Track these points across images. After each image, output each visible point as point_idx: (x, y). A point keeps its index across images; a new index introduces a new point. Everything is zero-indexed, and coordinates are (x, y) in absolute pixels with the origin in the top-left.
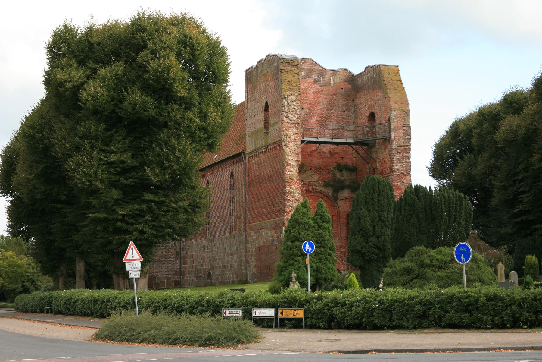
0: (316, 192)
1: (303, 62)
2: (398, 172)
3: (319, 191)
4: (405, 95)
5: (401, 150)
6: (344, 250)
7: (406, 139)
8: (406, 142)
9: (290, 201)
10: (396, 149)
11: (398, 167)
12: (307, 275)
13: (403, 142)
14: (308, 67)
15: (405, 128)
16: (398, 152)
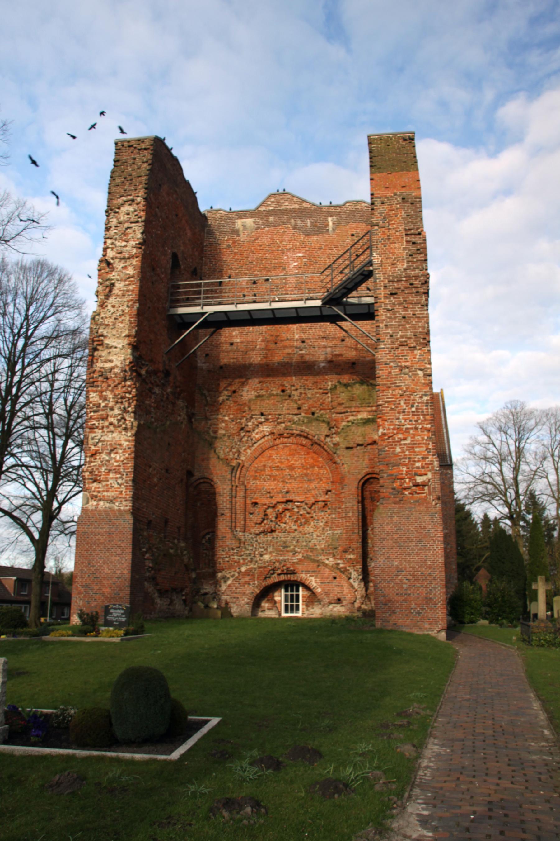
0: (292, 434)
1: (273, 200)
2: (393, 343)
3: (298, 432)
4: (417, 170)
5: (399, 289)
6: (352, 556)
7: (413, 262)
8: (414, 269)
9: (97, 427)
10: (385, 287)
11: (390, 331)
12: (303, 609)
13: (405, 270)
14: (283, 208)
15: (409, 238)
16: (392, 294)
